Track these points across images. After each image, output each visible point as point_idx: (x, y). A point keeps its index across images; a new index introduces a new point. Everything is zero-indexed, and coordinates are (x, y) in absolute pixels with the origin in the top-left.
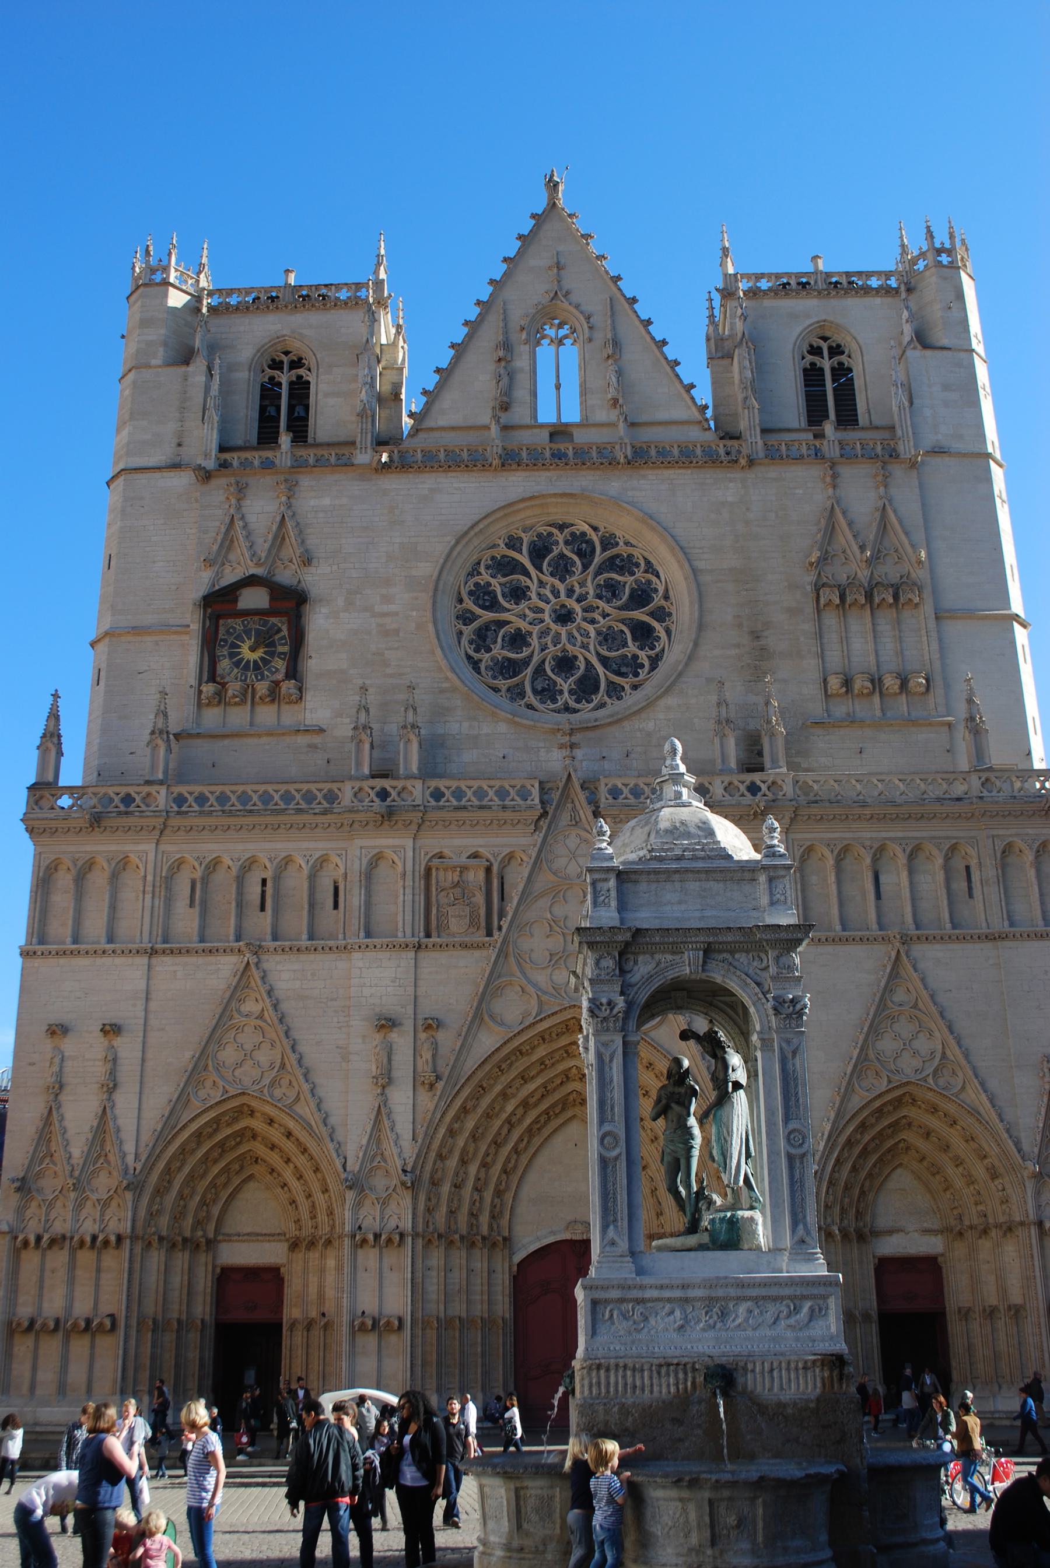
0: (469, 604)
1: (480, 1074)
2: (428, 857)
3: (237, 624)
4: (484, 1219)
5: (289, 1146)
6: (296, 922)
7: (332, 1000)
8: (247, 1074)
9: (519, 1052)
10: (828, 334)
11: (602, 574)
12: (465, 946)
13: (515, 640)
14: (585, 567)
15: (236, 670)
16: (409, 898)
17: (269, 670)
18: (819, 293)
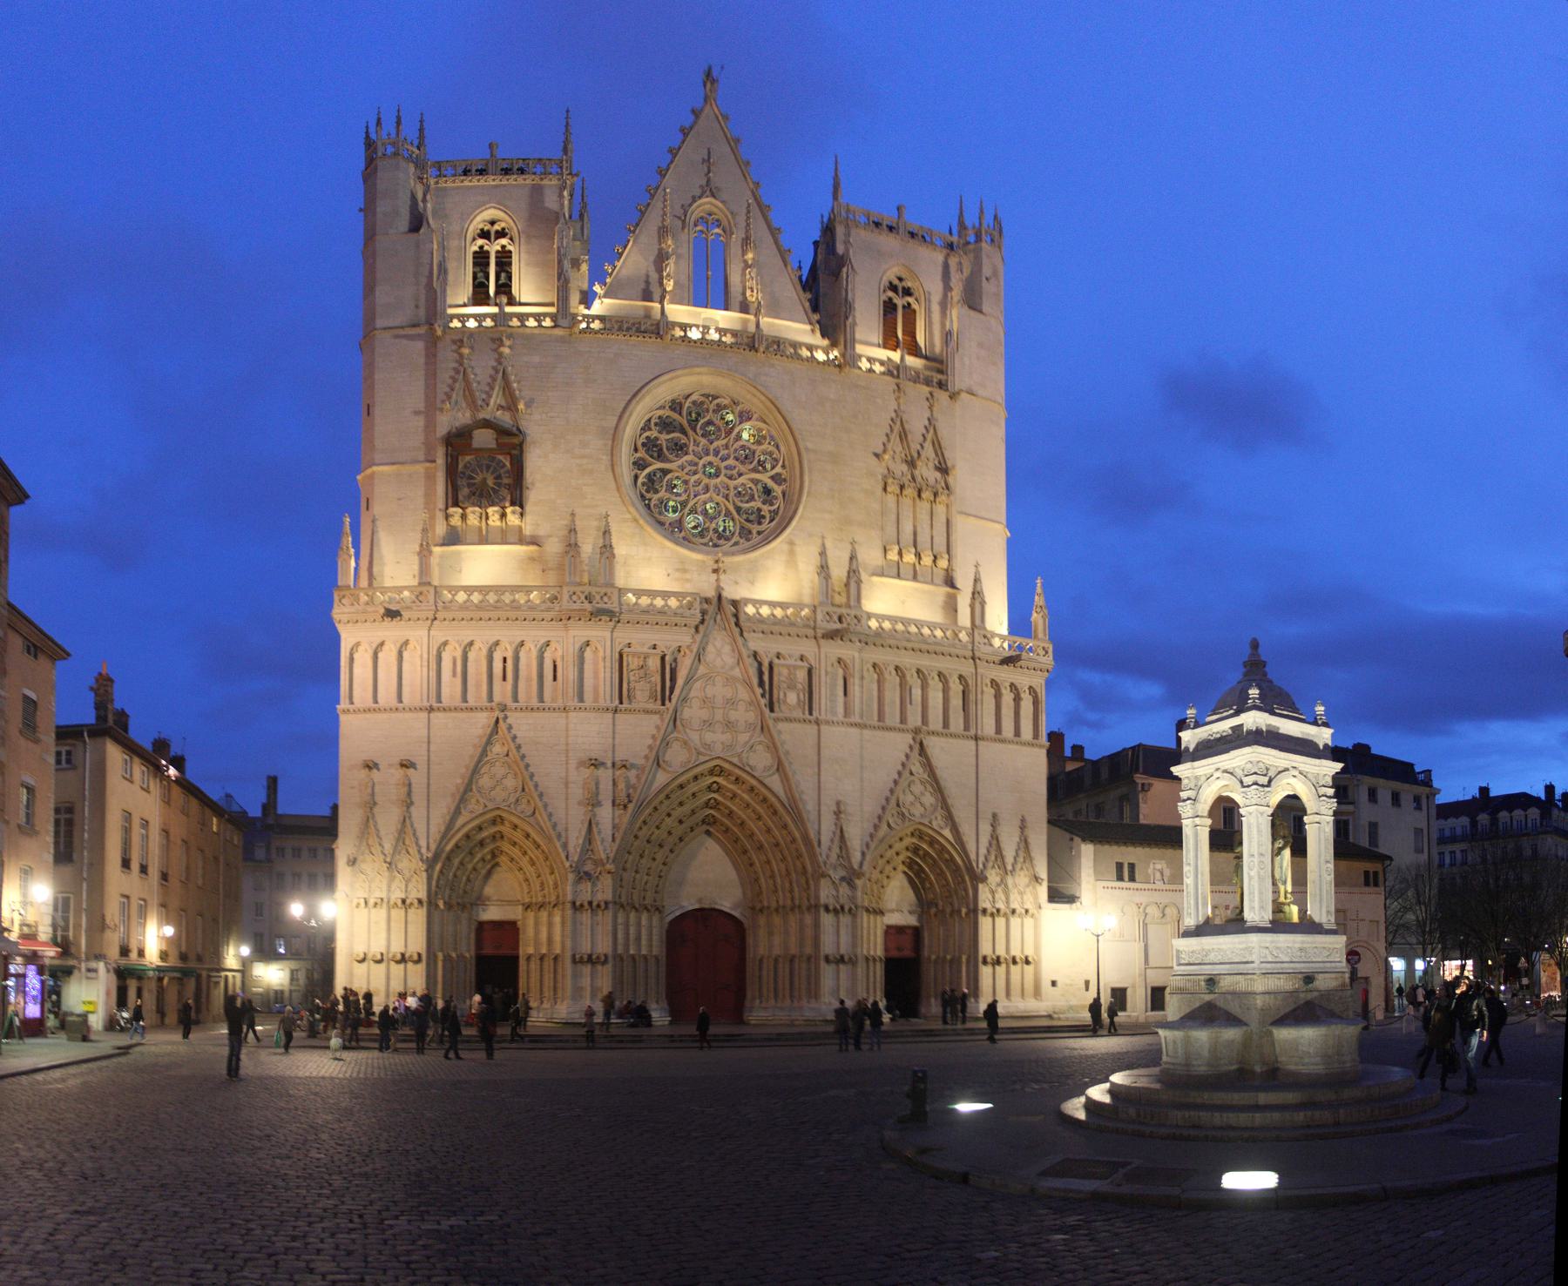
0: (641, 454)
5: (528, 844)
6: (528, 690)
8: (499, 794)
12: (647, 712)
16: (608, 675)
17: (498, 498)
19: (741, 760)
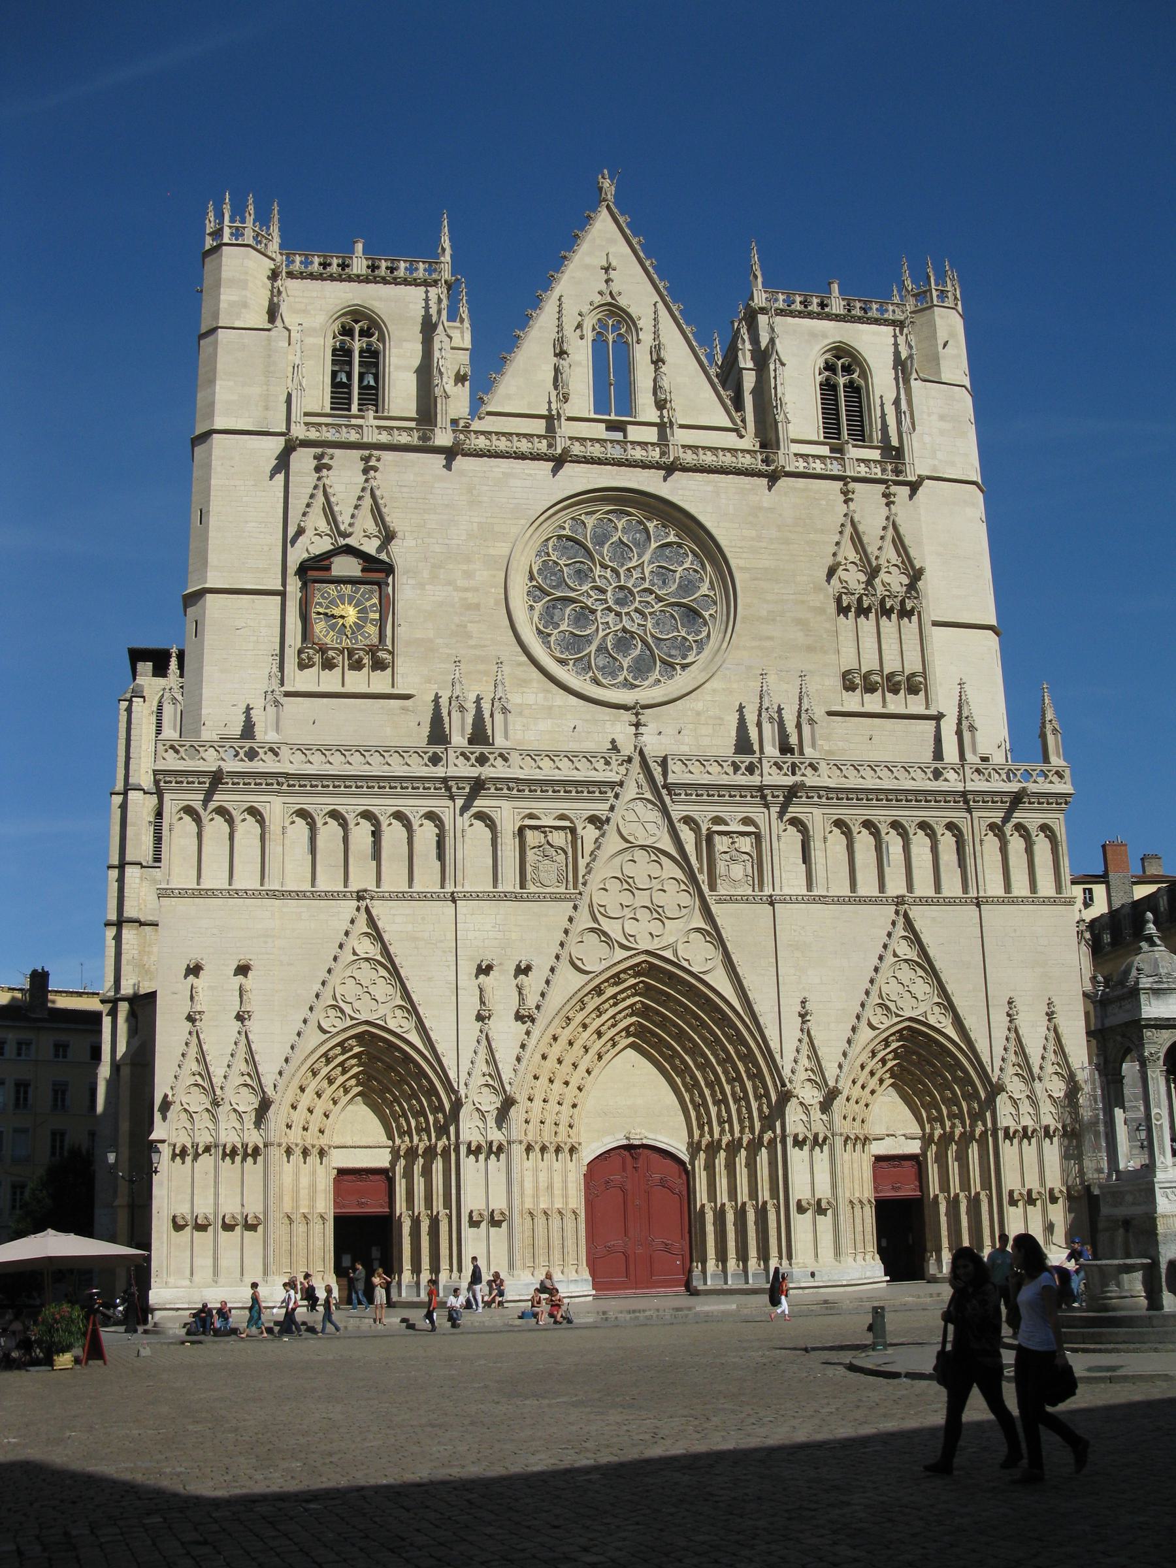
1: (568, 1007)
3: (332, 589)
4: (563, 1129)
7: (441, 941)
9: (598, 990)
10: (841, 354)
11: (653, 563)
12: (556, 898)
13: (579, 619)
14: (640, 556)
15: (332, 633)
18: (837, 316)
19: (676, 954)
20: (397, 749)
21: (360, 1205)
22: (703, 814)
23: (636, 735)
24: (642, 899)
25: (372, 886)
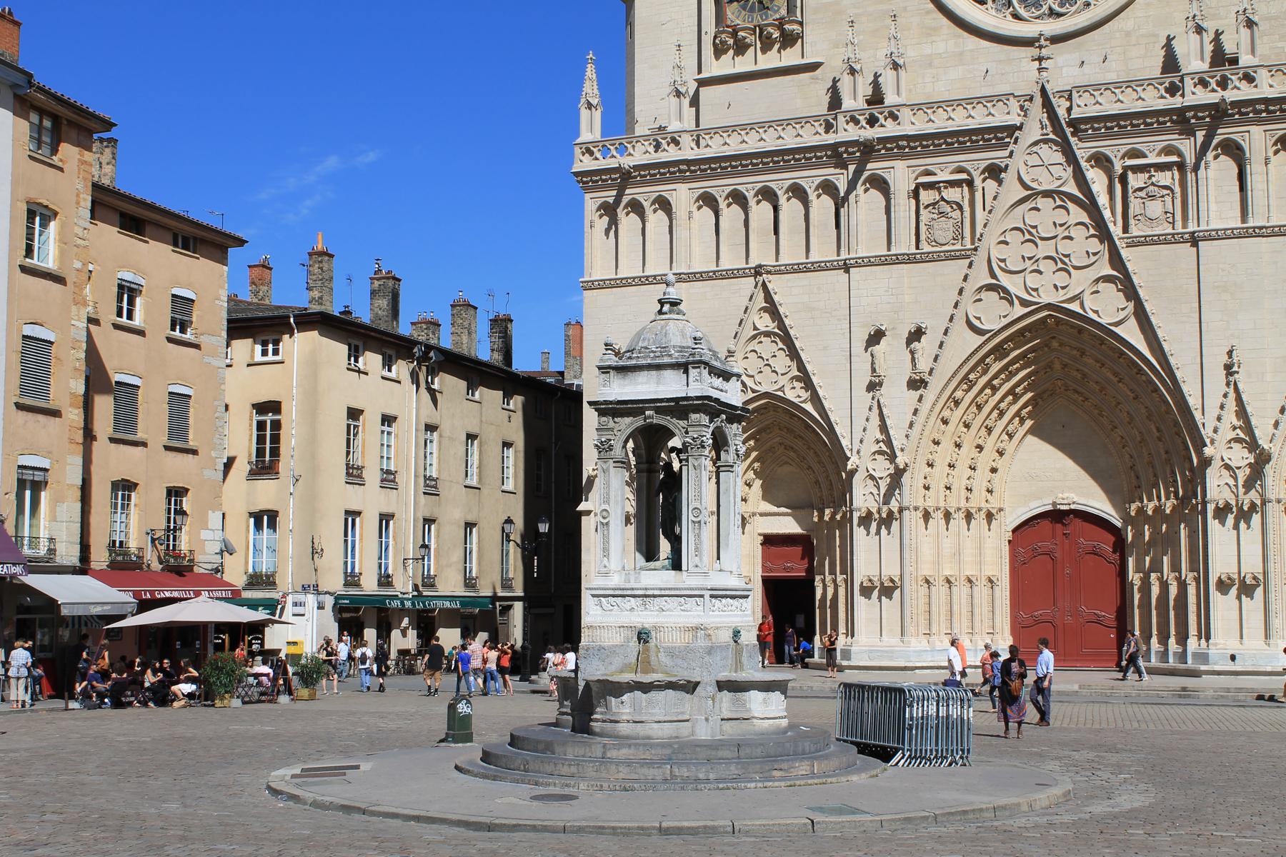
2: (914, 175)
20: (807, 119)
21: (785, 569)
22: (1115, 149)
23: (1040, 70)
24: (1045, 249)
25: (769, 261)
